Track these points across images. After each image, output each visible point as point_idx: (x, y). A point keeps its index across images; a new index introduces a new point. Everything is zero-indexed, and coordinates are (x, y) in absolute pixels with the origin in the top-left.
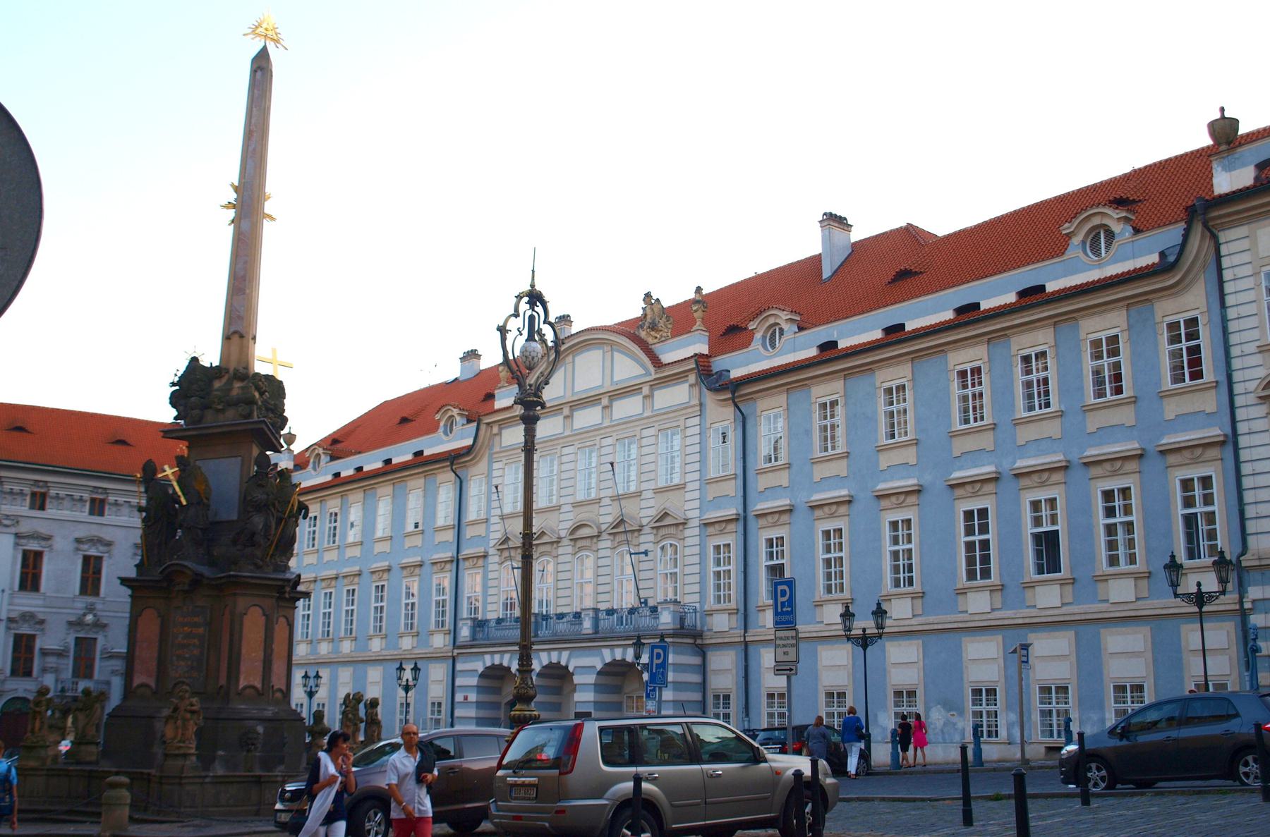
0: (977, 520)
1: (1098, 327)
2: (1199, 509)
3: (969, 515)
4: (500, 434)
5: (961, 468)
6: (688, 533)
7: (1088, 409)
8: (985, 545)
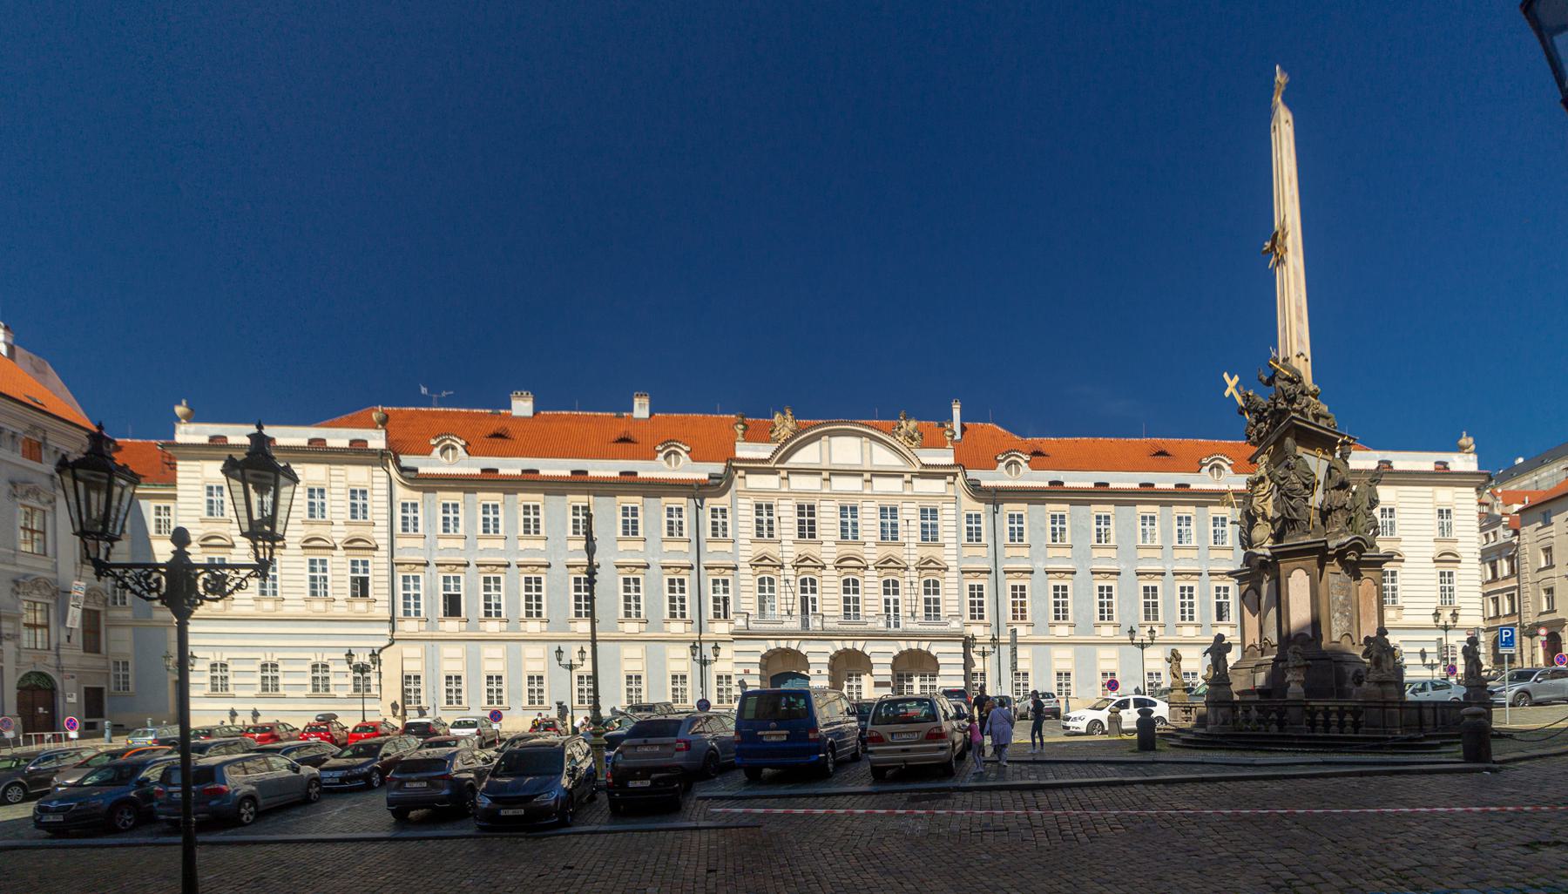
0: (1150, 592)
7: (1210, 548)
8: (1155, 605)
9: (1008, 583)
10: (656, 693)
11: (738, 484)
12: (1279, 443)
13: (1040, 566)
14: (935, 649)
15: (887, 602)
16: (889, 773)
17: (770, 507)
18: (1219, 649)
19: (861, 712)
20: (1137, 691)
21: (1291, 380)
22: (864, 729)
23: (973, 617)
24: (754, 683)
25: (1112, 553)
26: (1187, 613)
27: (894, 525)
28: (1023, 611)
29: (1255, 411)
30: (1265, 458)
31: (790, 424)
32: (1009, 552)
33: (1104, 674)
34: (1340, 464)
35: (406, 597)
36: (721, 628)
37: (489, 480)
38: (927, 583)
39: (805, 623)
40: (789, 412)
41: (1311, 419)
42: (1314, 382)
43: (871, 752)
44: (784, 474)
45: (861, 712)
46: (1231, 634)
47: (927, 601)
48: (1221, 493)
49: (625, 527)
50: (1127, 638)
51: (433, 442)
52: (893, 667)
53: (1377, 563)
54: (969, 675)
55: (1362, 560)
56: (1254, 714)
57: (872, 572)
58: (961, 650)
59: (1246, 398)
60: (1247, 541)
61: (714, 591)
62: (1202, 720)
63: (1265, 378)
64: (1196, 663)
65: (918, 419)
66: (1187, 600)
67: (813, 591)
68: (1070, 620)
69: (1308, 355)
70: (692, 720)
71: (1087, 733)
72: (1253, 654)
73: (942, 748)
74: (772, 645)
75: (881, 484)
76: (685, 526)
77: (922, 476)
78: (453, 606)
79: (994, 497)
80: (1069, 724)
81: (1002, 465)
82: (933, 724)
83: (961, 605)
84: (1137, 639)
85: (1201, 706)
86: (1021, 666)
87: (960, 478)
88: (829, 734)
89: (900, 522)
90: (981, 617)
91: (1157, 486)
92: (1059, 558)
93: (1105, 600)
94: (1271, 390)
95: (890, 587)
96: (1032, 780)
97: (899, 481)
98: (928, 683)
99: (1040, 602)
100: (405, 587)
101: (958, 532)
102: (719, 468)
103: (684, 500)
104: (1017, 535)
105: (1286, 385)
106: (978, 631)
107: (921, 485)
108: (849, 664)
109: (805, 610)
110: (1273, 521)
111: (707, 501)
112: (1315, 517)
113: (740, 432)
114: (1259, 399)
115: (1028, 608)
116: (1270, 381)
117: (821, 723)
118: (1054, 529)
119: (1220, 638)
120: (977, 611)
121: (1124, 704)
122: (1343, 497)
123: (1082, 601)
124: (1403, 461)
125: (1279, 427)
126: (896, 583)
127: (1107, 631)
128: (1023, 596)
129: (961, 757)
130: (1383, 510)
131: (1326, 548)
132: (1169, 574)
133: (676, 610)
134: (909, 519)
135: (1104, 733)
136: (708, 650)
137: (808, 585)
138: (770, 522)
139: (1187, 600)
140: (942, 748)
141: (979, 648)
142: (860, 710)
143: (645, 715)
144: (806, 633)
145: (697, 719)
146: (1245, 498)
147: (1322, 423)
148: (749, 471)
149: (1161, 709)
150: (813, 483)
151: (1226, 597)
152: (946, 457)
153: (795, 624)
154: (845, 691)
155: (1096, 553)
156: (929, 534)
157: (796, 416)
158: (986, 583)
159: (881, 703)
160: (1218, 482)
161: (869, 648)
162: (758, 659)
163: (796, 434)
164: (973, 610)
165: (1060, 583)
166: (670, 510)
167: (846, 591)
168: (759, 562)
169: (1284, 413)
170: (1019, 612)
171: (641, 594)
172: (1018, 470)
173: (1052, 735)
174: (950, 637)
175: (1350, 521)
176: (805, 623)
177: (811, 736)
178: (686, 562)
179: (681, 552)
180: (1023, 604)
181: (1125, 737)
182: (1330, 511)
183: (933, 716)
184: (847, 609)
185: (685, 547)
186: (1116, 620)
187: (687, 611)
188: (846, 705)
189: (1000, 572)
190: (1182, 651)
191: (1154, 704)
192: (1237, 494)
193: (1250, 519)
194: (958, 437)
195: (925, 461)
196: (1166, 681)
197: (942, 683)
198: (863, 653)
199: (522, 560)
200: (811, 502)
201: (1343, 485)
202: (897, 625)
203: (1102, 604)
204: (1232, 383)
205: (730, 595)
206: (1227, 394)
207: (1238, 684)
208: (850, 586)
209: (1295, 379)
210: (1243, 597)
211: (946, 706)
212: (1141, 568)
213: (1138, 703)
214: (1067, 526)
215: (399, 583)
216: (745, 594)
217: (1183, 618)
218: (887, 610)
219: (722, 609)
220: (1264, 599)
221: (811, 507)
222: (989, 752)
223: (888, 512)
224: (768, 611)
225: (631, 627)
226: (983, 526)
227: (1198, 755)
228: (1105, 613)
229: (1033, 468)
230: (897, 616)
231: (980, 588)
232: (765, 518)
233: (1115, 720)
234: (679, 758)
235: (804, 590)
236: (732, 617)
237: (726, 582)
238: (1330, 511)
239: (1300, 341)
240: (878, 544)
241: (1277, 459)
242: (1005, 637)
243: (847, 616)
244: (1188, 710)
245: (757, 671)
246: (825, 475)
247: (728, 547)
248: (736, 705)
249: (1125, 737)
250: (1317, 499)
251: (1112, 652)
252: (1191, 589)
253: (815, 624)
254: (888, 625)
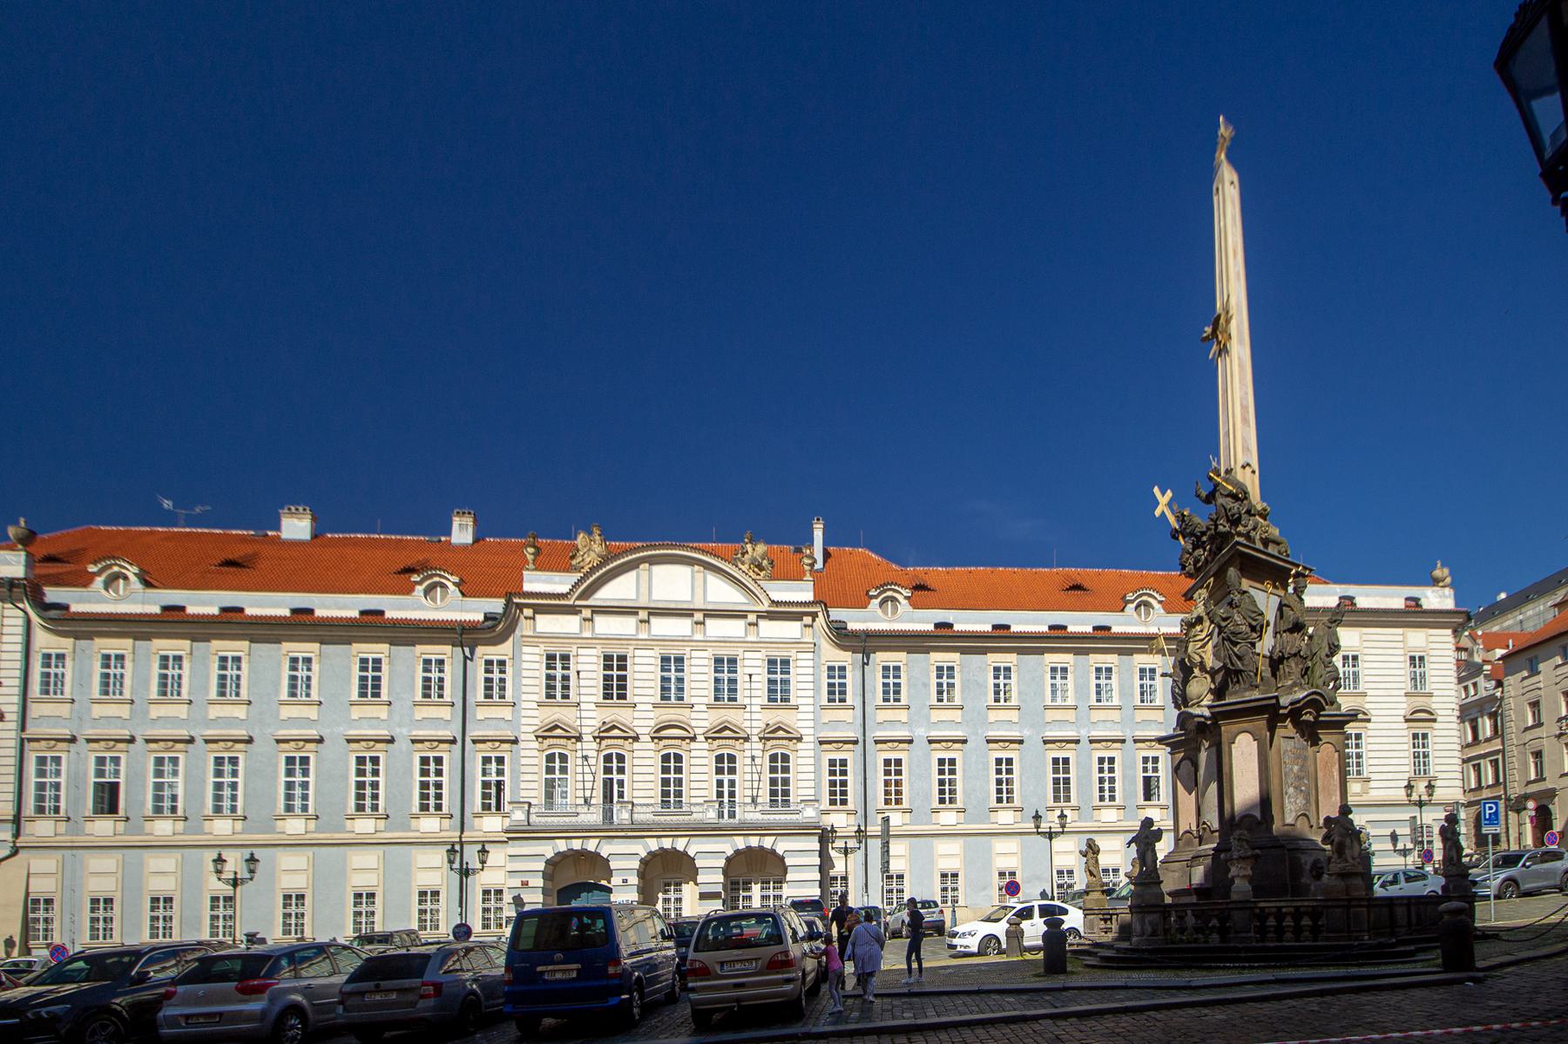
0: (1061, 764)
1: (1141, 660)
3: (1056, 761)
6: (800, 745)
9: (879, 757)
10: (396, 917)
11: (524, 628)
12: (1220, 574)
13: (921, 733)
14: (782, 846)
15: (720, 783)
16: (716, 1017)
17: (565, 658)
18: (1146, 837)
19: (680, 935)
20: (1044, 895)
21: (1235, 497)
22: (683, 958)
23: (833, 802)
24: (535, 899)
25: (1013, 715)
26: (1107, 791)
27: (733, 681)
28: (898, 793)
29: (1192, 534)
30: (1203, 593)
31: (598, 548)
32: (882, 716)
33: (1002, 874)
34: (1293, 601)
35: (41, 787)
36: (492, 824)
37: (173, 621)
38: (773, 758)
39: (608, 815)
40: (596, 531)
41: (1259, 546)
42: (1263, 498)
43: (693, 990)
44: (587, 613)
45: (680, 935)
46: (1160, 817)
47: (773, 782)
48: (1150, 638)
49: (363, 687)
50: (1031, 825)
51: (92, 569)
52: (725, 872)
53: (1339, 724)
54: (826, 880)
55: (1320, 721)
56: (1190, 920)
57: (701, 745)
58: (817, 846)
59: (1181, 518)
60: (1181, 698)
61: (484, 774)
62: (1125, 930)
63: (1204, 494)
64: (1117, 856)
65: (768, 542)
66: (1106, 775)
67: (621, 770)
68: (959, 804)
69: (1256, 466)
70: (445, 954)
71: (979, 954)
72: (1189, 843)
73: (788, 981)
74: (562, 846)
75: (716, 627)
76: (447, 684)
77: (771, 616)
78: (108, 799)
79: (865, 644)
80: (956, 941)
81: (876, 602)
82: (778, 948)
83: (817, 787)
84: (1044, 827)
85: (1124, 912)
86: (896, 866)
87: (821, 619)
88: (636, 967)
89: (741, 677)
90: (844, 802)
91: (1071, 629)
92: (946, 722)
93: (1004, 776)
94: (1211, 508)
95: (725, 764)
96: (907, 1019)
97: (741, 623)
98: (771, 893)
99: (920, 780)
100: (41, 773)
101: (816, 690)
102: (496, 605)
103: (448, 649)
104: (892, 693)
105: (1229, 503)
106: (840, 821)
107: (769, 629)
108: (667, 869)
109: (608, 797)
110: (1213, 673)
111: (480, 650)
112: (1264, 667)
113: (530, 558)
114: (1197, 520)
115: (905, 788)
116: (1210, 498)
117: (625, 951)
118: (940, 685)
119: (1148, 822)
120: (838, 794)
121: (1026, 913)
122: (1298, 642)
123: (974, 779)
124: (1369, 597)
125: (1222, 555)
126: (732, 759)
127: (1006, 818)
128: (899, 773)
129: (814, 992)
130: (1345, 658)
131: (1277, 706)
132: (1085, 742)
133: (430, 800)
134: (753, 668)
135: (1001, 952)
136: (471, 856)
137: (614, 763)
138: (566, 678)
139: (1106, 775)
140: (788, 981)
141: (839, 844)
142: (679, 932)
143: (377, 949)
144: (609, 829)
145: (452, 953)
146: (1179, 643)
147: (1272, 549)
149: (1074, 918)
151: (1155, 770)
152: (802, 592)
153: (594, 817)
154: (659, 906)
155: (993, 716)
156: (778, 693)
157: (606, 537)
158: (850, 756)
159: (708, 921)
160: (1145, 623)
161: (694, 847)
162: (541, 866)
163: (605, 560)
164: (833, 793)
165: (947, 755)
166: (427, 662)
167: (665, 770)
168: (548, 732)
169: (1227, 536)
170: (894, 794)
171: (381, 779)
172: (895, 609)
173: (934, 957)
174: (802, 830)
175: (1306, 672)
176: (608, 815)
177: (611, 970)
178: (446, 733)
179: (439, 719)
180: (898, 783)
181: (1028, 956)
182: (1281, 660)
183: (777, 937)
184: (665, 794)
185: (445, 713)
186: (1017, 803)
187: (445, 802)
188: (660, 926)
189: (870, 742)
190: (1101, 842)
191: (1065, 912)
192: (1169, 638)
193: (1185, 670)
194: (819, 565)
195: (776, 596)
196: (1080, 881)
197: (789, 892)
198: (685, 854)
199: (211, 732)
200: (622, 652)
201: (1298, 627)
202: (732, 815)
203: (999, 782)
204: (1164, 499)
205: (506, 778)
206: (1157, 513)
207: (1171, 882)
208: (672, 763)
209: (1240, 496)
210: (1176, 770)
211: (795, 922)
213: (1045, 911)
214: (957, 681)
215: (31, 767)
216: (526, 776)
217: (1102, 799)
218: (720, 794)
219: (494, 797)
220: (1202, 771)
221: (623, 658)
222: (850, 983)
223: (725, 664)
224: (558, 800)
225: (365, 826)
226: (848, 681)
227: (1120, 978)
228: (1004, 793)
229: (915, 606)
230: (732, 803)
231: (844, 763)
232: (559, 673)
233: (1015, 934)
234: (425, 1007)
235: (608, 770)
236: (507, 808)
237: (500, 761)
238: (1281, 660)
239: (1246, 449)
240: (710, 707)
241: (1218, 594)
242: (875, 828)
243: (665, 804)
244: (1107, 919)
245: (538, 882)
246: (643, 615)
247: (507, 713)
248: (508, 931)
249: (1028, 956)
250: (1266, 644)
251: (1012, 845)
252: (1111, 760)
253: (621, 815)
254: (721, 815)
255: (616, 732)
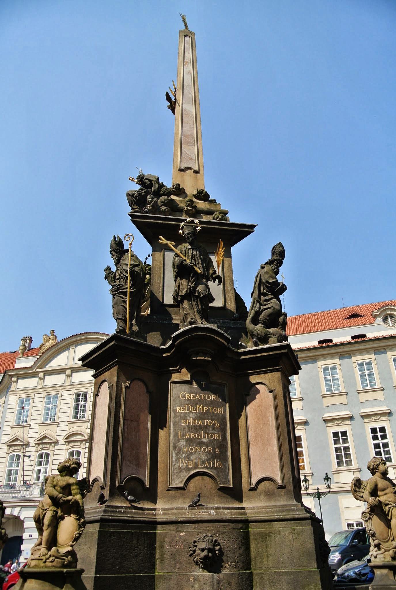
2: (380, 441)
4: (17, 382)
5: (329, 412)
8: (347, 449)
44: (41, 375)
148: (20, 377)
150: (59, 379)
212: (328, 415)
246: (68, 372)
255: (47, 440)
